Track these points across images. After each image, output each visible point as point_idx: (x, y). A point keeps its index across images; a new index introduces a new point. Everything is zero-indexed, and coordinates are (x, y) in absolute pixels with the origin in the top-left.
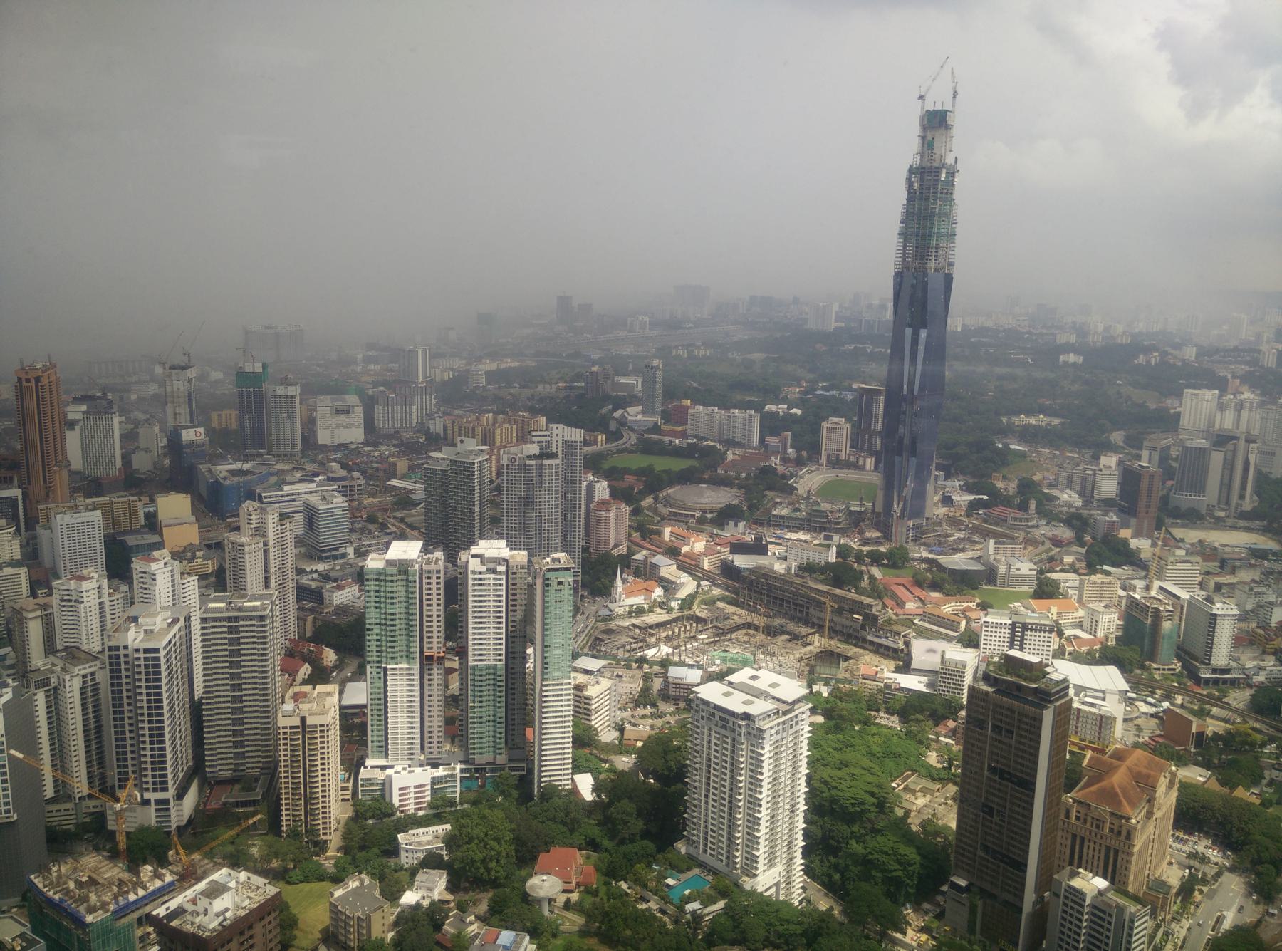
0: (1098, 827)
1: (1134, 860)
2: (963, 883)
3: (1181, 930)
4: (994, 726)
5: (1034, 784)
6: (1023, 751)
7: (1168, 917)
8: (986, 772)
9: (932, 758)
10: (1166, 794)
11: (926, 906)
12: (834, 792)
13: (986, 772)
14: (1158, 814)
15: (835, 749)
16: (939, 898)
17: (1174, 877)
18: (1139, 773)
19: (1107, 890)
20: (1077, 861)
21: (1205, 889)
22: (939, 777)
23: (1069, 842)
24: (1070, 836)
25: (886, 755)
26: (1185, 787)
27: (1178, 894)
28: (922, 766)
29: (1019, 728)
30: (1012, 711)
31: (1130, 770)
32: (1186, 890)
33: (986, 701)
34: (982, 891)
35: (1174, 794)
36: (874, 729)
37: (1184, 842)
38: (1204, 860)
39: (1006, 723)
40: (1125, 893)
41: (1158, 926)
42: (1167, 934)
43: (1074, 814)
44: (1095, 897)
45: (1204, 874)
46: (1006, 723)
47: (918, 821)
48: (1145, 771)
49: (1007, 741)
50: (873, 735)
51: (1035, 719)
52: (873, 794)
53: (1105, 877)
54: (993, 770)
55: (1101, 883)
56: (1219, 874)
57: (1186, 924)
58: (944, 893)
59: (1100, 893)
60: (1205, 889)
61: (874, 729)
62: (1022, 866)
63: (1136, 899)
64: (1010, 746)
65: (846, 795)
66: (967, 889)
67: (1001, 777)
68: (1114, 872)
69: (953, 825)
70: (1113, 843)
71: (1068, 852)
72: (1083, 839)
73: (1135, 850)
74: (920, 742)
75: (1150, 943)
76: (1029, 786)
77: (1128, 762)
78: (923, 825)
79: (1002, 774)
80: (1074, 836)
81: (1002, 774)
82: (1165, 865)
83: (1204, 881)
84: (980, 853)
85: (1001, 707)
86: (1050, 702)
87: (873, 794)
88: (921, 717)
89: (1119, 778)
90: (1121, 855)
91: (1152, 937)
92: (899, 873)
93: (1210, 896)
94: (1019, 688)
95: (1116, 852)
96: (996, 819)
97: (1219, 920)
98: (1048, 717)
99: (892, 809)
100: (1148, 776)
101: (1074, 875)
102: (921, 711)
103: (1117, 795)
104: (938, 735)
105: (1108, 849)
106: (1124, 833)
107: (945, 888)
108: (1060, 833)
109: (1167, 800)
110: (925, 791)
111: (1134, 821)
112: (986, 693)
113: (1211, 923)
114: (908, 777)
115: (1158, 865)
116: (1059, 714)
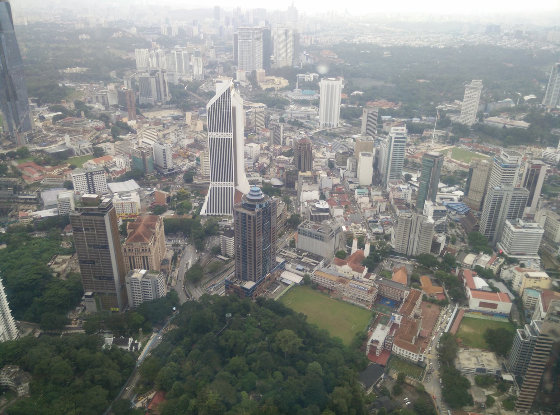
1: (153, 257)
2: (90, 294)
3: (175, 274)
4: (86, 229)
5: (108, 246)
6: (100, 235)
7: (170, 271)
8: (87, 248)
9: (65, 245)
10: (160, 228)
11: (78, 308)
12: (20, 281)
13: (87, 248)
14: (159, 237)
15: (16, 259)
16: (82, 303)
17: (169, 255)
18: (148, 225)
19: (146, 273)
20: (133, 266)
21: (181, 255)
22: (70, 252)
23: (129, 260)
24: (128, 258)
25: (42, 252)
26: (165, 220)
27: (172, 261)
28: (61, 250)
29: (96, 226)
30: (91, 220)
31: (144, 225)
32: (175, 258)
33: (80, 220)
34: (99, 293)
35: (163, 226)
36: (33, 242)
37: (170, 240)
38: (178, 245)
39: (90, 226)
40: (153, 272)
41: (168, 276)
42: (171, 278)
43: (127, 250)
44: (143, 278)
45: (179, 250)
46: (90, 226)
47: (65, 275)
48: (150, 223)
49: (93, 233)
50: (34, 244)
51: (101, 221)
52: (39, 274)
53: (145, 269)
54: (89, 246)
55: (143, 271)
56: (184, 248)
57: (177, 271)
58: (84, 300)
59: (144, 276)
60: (181, 255)
61: (33, 242)
62: (111, 278)
63: (157, 272)
64: (94, 234)
65: (25, 280)
66: (92, 295)
67: (94, 248)
68: (148, 267)
69: (79, 271)
70: (144, 254)
71: (129, 263)
72: (133, 257)
73: (153, 254)
74: (57, 240)
75: (166, 283)
76: (106, 247)
77: (143, 222)
78: (67, 277)
79: (94, 246)
80: (130, 258)
81: (94, 246)
82: (166, 252)
83: (180, 252)
84: (94, 280)
85: (86, 220)
86: (106, 212)
87: (39, 274)
88: (55, 228)
89: (140, 229)
90: (148, 258)
91: (166, 281)
92: (61, 302)
93: (182, 257)
94: (92, 210)
95: (147, 257)
96: (97, 265)
97: (187, 264)
98: (107, 218)
99: (51, 276)
100: (151, 225)
101: (132, 274)
102: (54, 226)
103: (142, 236)
104: (65, 233)
105: (143, 257)
106: (148, 250)
107: (83, 298)
108: (124, 258)
109: (159, 229)
110: (64, 261)
111: (150, 244)
112: (78, 217)
113: (185, 266)
114: (56, 257)
115: (163, 254)
116: (111, 215)
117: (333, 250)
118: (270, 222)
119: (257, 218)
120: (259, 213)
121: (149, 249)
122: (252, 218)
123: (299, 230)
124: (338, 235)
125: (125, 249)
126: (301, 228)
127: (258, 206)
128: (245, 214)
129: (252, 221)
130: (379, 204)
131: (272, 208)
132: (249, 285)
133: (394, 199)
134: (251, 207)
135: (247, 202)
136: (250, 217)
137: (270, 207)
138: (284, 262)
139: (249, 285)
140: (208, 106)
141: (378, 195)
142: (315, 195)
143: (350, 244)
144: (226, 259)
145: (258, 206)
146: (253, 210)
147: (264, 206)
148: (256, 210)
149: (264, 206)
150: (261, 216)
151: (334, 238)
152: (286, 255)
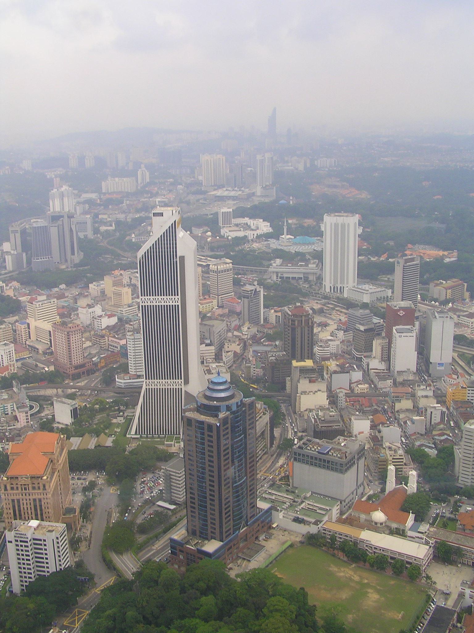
0: (25, 489)
68: (42, 514)
71: (12, 511)
117: (355, 487)
118: (245, 437)
119: (222, 428)
120: (225, 421)
121: (44, 486)
122: (214, 429)
123: (295, 454)
124: (362, 462)
125: (6, 487)
126: (300, 451)
127: (223, 408)
128: (202, 423)
129: (214, 434)
130: (429, 411)
131: (248, 413)
132: (211, 546)
133: (455, 402)
134: (213, 411)
135: (206, 402)
136: (210, 427)
137: (245, 412)
138: (270, 509)
139: (211, 546)
140: (141, 253)
141: (426, 397)
142: (322, 399)
143: (383, 478)
144: (172, 507)
145: (223, 408)
146: (217, 416)
147: (234, 408)
148: (221, 415)
149: (234, 408)
150: (229, 425)
151: (354, 468)
152: (273, 497)
